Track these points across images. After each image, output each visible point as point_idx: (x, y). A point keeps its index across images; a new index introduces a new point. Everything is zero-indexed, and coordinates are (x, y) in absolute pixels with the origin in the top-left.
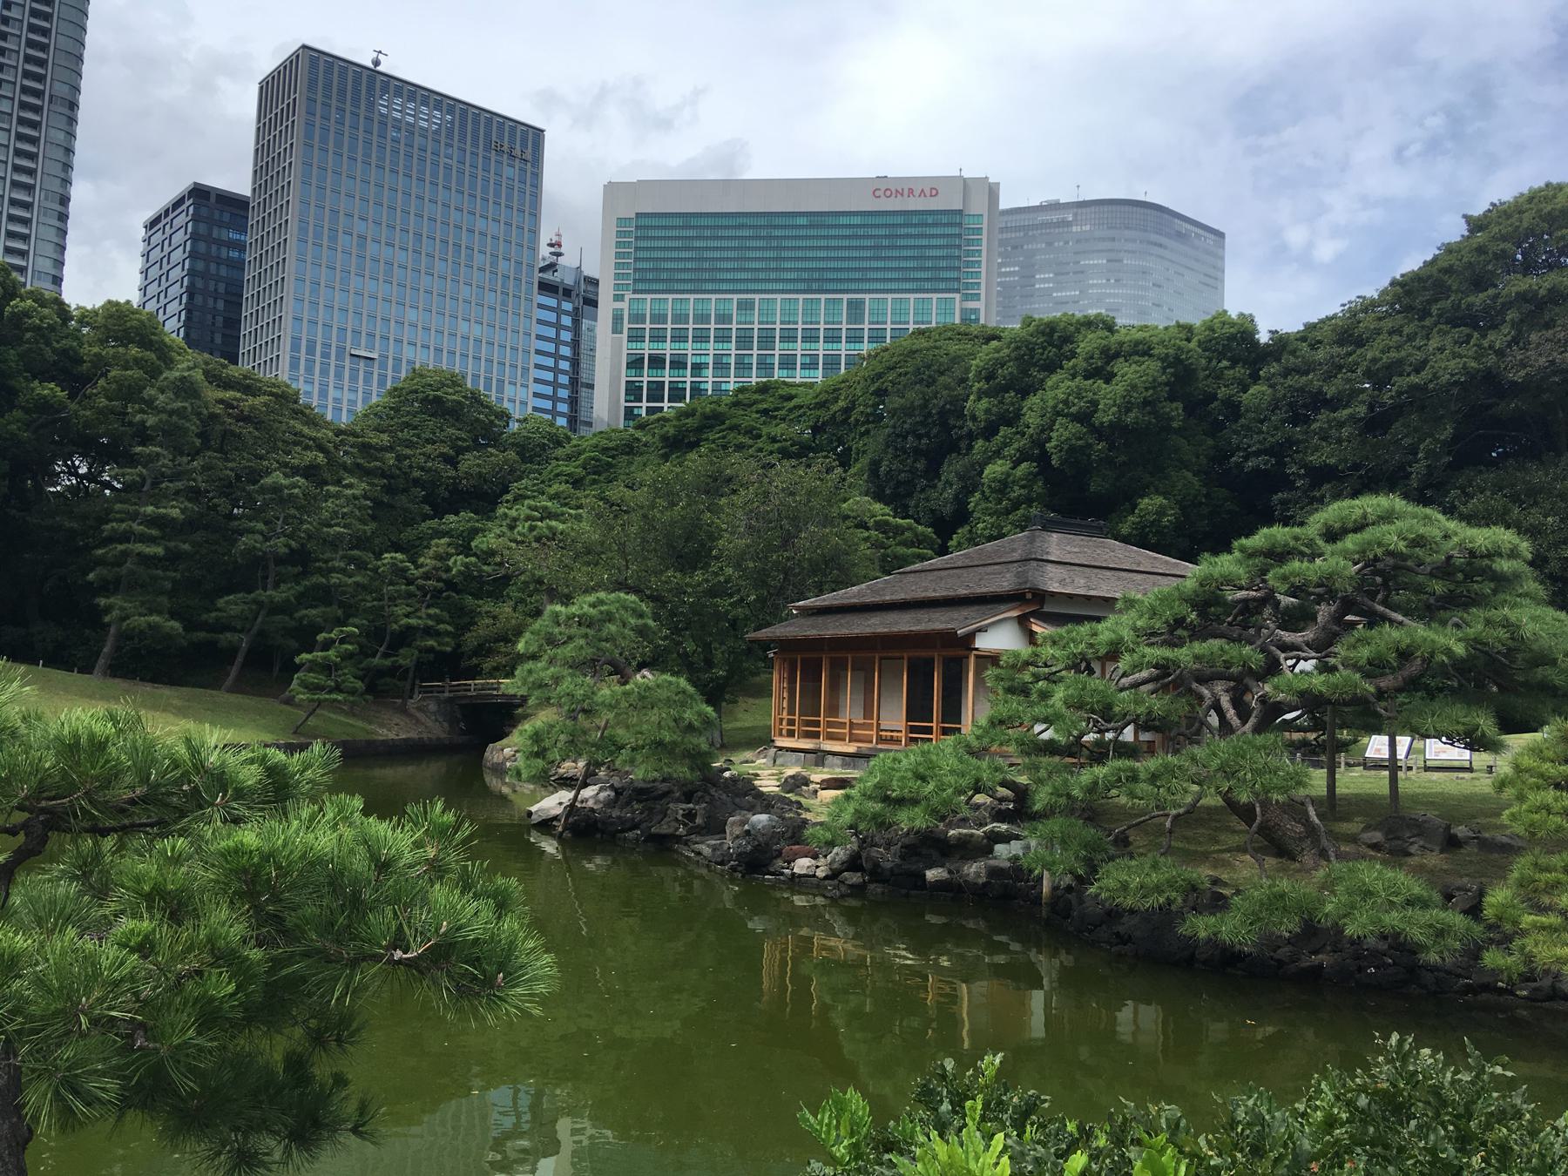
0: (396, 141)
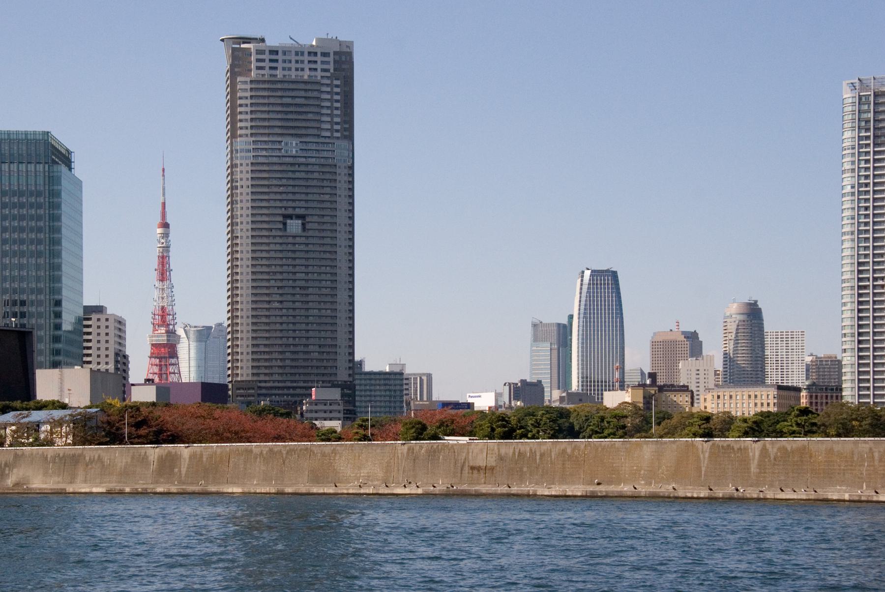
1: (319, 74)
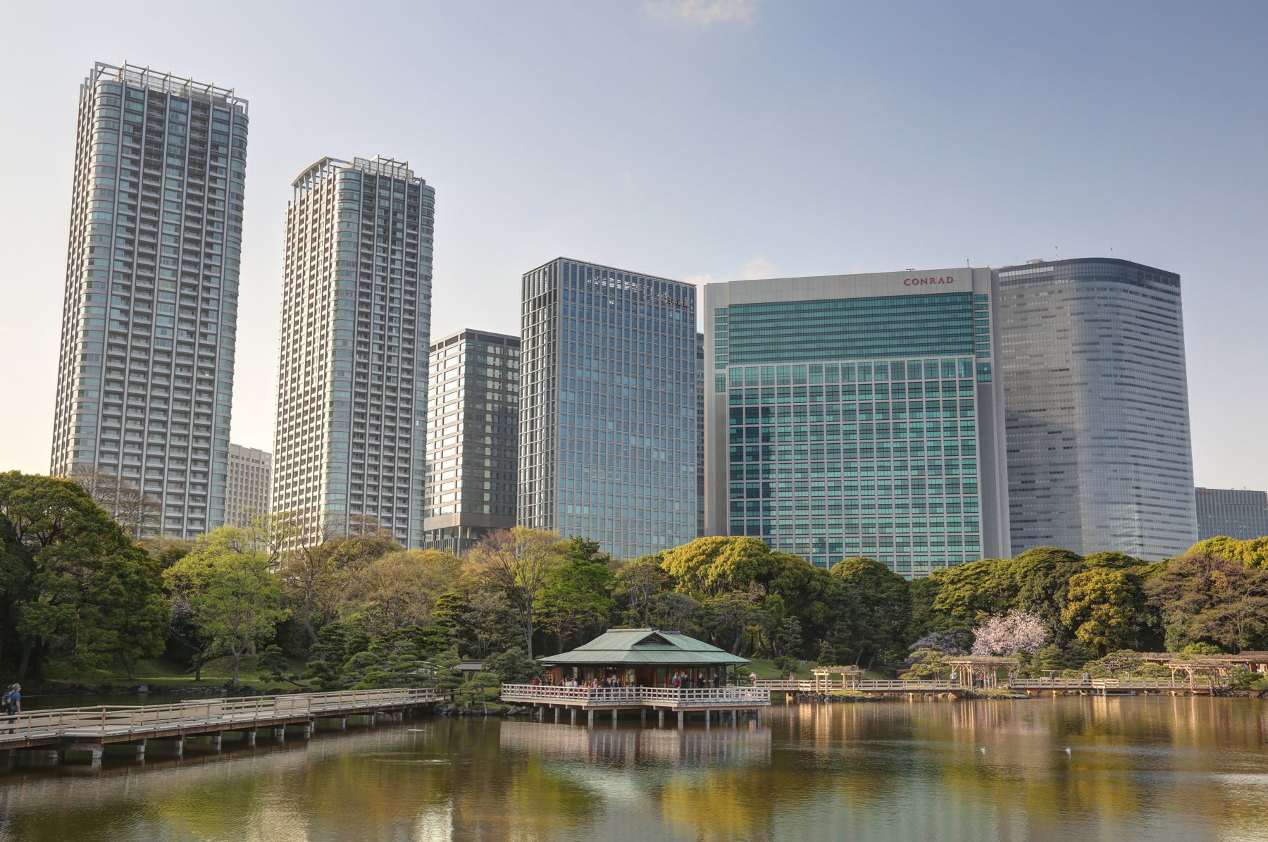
0: (612, 307)
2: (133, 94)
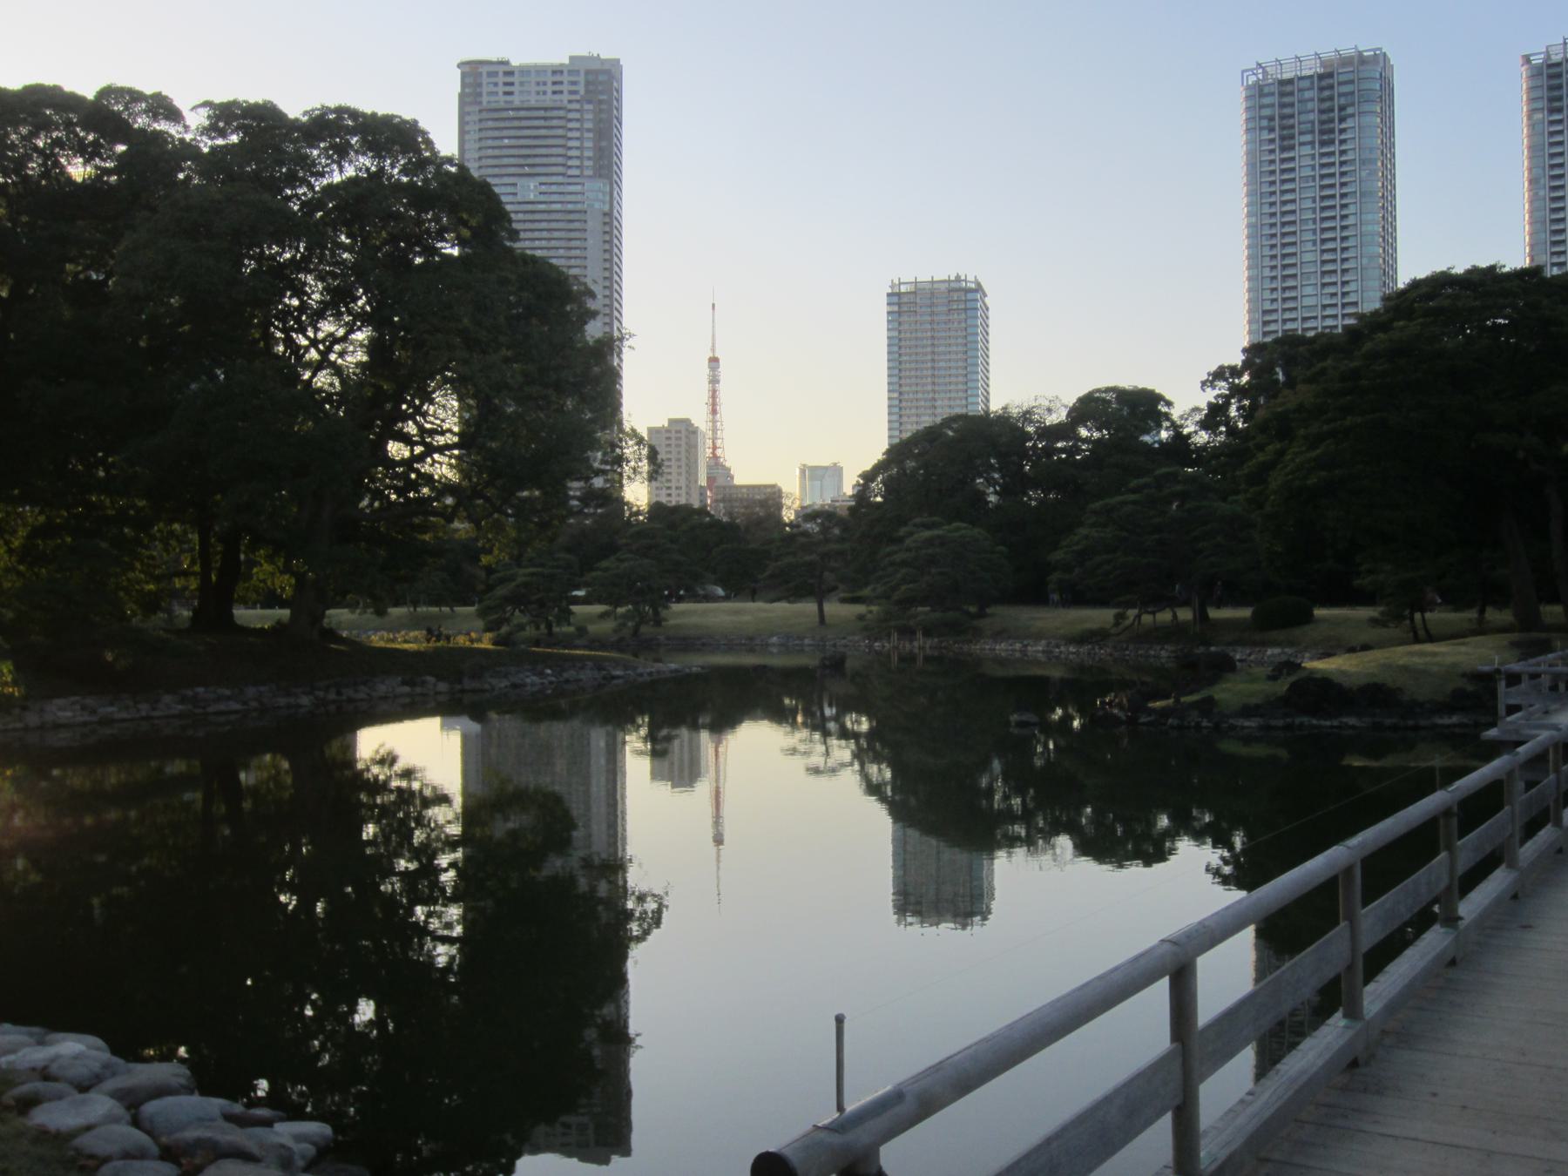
1: (565, 97)
2: (1266, 90)
